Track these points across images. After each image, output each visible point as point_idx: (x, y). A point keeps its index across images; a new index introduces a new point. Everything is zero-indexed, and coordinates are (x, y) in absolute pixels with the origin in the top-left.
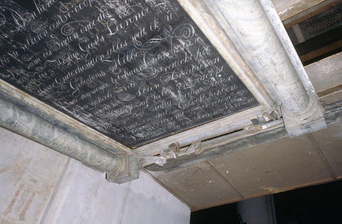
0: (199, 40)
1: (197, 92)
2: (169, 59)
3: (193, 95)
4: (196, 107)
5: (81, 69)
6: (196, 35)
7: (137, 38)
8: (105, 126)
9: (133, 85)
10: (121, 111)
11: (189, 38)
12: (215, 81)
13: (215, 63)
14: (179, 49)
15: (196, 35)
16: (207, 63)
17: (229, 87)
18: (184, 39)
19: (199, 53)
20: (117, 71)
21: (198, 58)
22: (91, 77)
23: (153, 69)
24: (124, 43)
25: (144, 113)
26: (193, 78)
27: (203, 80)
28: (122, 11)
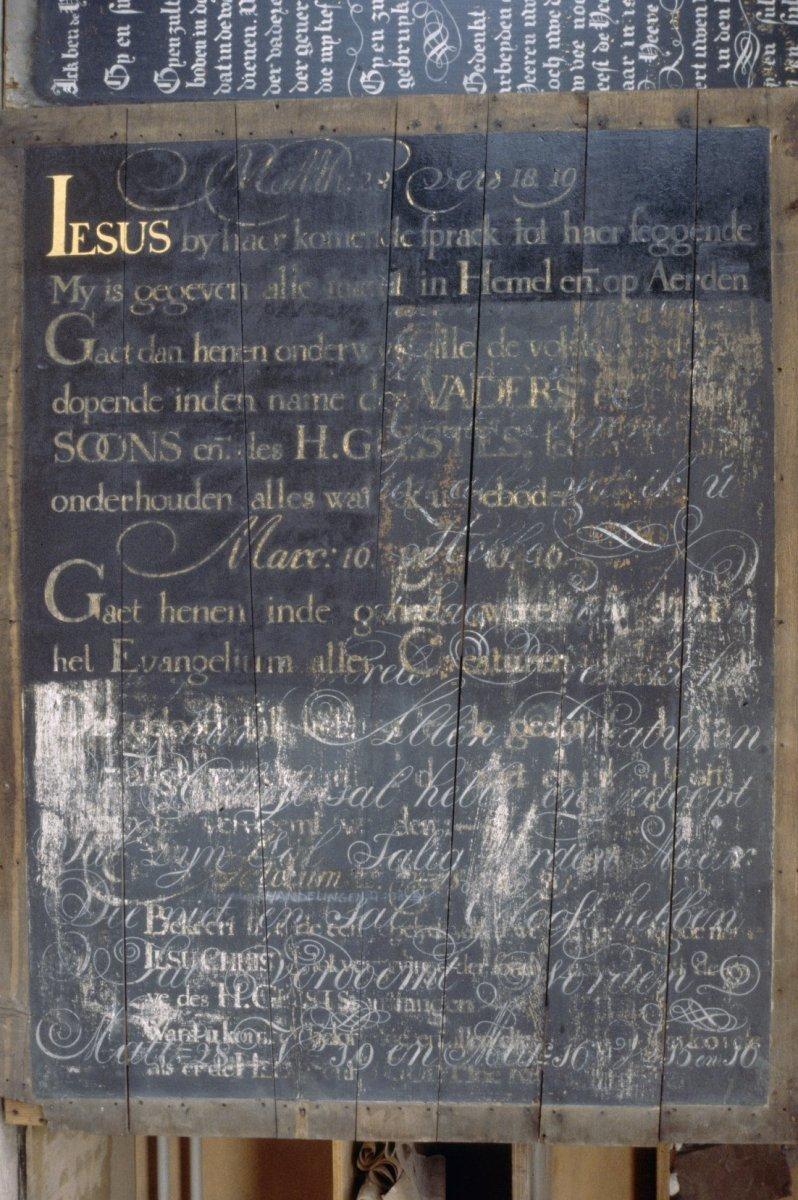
0: (749, 616)
1: (586, 864)
6: (749, 593)
11: (722, 592)
12: (684, 843)
13: (736, 747)
15: (749, 593)
17: (712, 909)
18: (706, 589)
19: (716, 669)
20: (414, 575)
23: (533, 642)
26: (622, 780)
27: (652, 808)
28: (616, 385)
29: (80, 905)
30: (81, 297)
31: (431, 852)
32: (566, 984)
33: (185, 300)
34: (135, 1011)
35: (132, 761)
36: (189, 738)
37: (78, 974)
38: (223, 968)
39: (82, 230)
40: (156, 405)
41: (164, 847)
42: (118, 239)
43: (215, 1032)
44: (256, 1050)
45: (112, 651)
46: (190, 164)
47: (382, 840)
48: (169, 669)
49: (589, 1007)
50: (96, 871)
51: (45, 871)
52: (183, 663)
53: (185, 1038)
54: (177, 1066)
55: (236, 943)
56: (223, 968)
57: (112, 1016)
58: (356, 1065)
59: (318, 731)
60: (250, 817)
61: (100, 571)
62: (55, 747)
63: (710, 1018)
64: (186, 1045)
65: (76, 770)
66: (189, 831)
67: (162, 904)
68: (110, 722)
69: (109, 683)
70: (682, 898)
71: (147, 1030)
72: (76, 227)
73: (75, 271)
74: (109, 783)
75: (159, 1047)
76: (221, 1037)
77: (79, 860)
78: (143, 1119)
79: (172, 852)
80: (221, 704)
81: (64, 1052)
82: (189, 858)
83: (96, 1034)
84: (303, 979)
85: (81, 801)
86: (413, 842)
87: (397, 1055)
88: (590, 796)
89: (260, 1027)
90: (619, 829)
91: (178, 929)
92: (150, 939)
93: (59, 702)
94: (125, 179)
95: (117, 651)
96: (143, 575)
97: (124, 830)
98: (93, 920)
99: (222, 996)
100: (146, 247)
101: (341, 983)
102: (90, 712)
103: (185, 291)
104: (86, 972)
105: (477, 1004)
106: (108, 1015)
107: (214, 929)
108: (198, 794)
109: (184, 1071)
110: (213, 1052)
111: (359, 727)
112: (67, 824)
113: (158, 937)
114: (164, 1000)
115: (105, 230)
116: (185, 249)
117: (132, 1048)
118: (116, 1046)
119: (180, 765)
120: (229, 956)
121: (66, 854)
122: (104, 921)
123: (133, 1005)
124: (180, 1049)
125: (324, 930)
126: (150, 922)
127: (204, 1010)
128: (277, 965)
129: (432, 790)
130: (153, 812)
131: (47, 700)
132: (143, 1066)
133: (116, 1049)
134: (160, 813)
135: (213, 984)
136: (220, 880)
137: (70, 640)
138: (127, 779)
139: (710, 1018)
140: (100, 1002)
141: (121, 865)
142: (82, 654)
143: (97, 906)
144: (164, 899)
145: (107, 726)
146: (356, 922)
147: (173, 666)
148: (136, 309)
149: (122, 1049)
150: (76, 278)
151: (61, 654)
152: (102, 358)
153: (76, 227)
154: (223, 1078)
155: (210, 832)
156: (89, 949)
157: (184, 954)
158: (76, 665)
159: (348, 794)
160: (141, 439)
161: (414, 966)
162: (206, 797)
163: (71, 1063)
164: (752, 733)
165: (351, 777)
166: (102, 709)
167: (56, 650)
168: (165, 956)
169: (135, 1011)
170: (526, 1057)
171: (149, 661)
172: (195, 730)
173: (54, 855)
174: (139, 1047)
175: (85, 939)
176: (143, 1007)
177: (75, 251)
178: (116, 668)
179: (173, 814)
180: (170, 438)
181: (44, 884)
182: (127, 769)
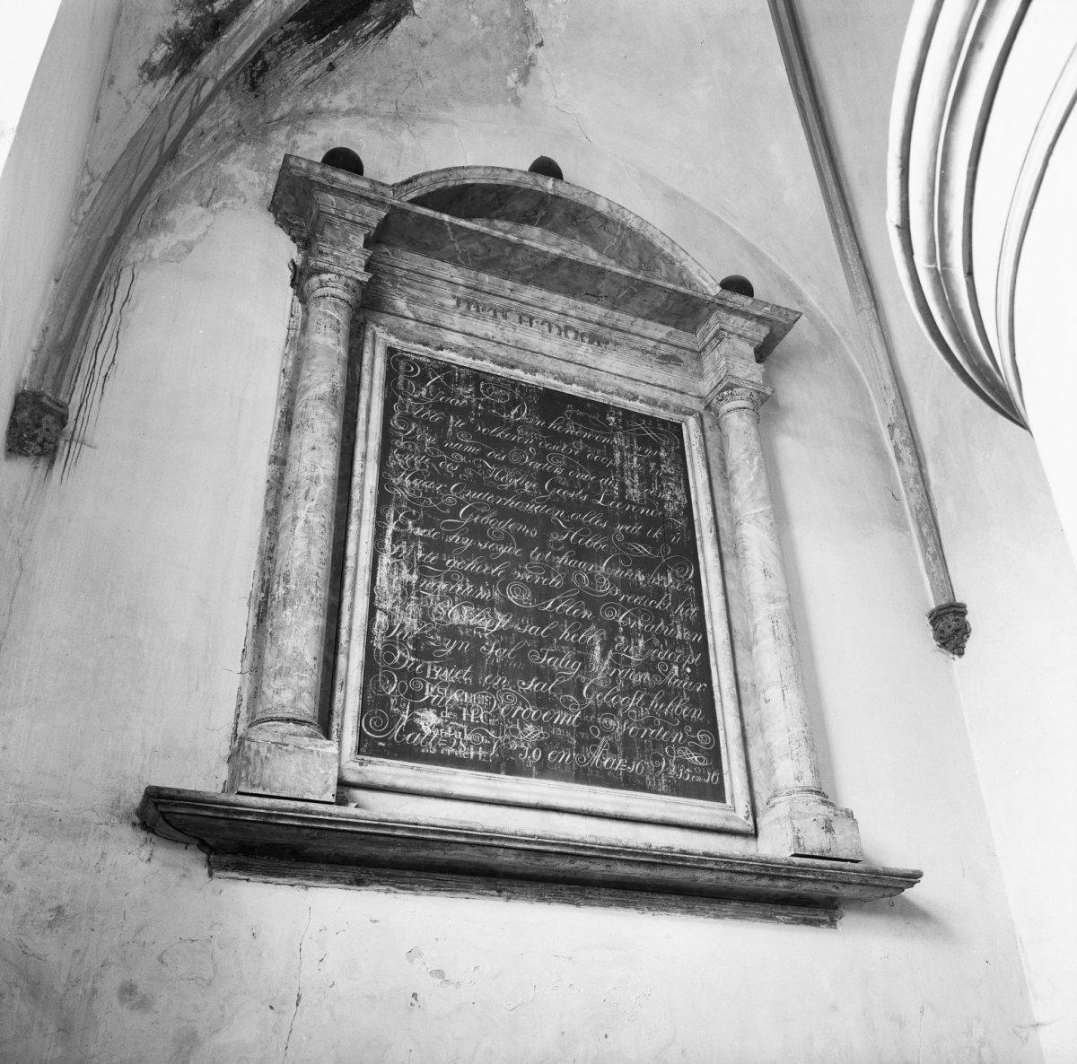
1: (636, 678)
2: (639, 585)
3: (627, 681)
4: (612, 718)
5: (511, 503)
7: (623, 530)
8: (403, 625)
9: (554, 583)
10: (478, 615)
14: (662, 582)
16: (683, 632)
18: (674, 575)
20: (557, 544)
21: (676, 615)
22: (510, 524)
24: (603, 522)
25: (512, 655)
26: (649, 645)
31: (566, 661)
32: (631, 731)
36: (453, 590)
37: (389, 693)
41: (439, 638)
44: (482, 745)
47: (545, 651)
49: (642, 746)
54: (439, 749)
55: (474, 688)
58: (532, 759)
59: (514, 599)
60: (482, 631)
63: (696, 758)
66: (451, 632)
68: (415, 577)
70: (677, 701)
71: (423, 727)
74: (412, 604)
75: (429, 737)
76: (463, 736)
77: (394, 637)
79: (442, 641)
82: (451, 644)
84: (506, 712)
85: (397, 608)
86: (559, 655)
87: (553, 756)
88: (635, 649)
89: (484, 733)
90: (648, 665)
92: (428, 679)
97: (419, 626)
99: (464, 714)
101: (525, 717)
102: (405, 571)
105: (590, 736)
106: (403, 716)
107: (462, 680)
110: (459, 744)
111: (533, 601)
112: (389, 618)
117: (415, 736)
118: (407, 734)
120: (469, 694)
122: (405, 668)
125: (516, 689)
126: (429, 672)
128: (493, 704)
129: (566, 634)
139: (696, 758)
141: (416, 642)
146: (532, 687)
149: (410, 736)
159: (528, 629)
161: (560, 713)
163: (381, 740)
164: (699, 636)
165: (530, 621)
168: (436, 690)
170: (615, 765)
176: (422, 715)
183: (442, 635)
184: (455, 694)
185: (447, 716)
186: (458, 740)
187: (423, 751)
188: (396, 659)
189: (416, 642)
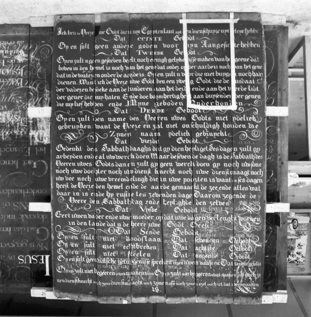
29: (39, 86)
30: (41, 245)
33: (14, 243)
34: (26, 58)
35: (25, 124)
36: (10, 130)
38: (3, 70)
39: (41, 261)
40: (20, 216)
41: (17, 102)
42: (32, 259)
43: (6, 53)
45: (30, 153)
46: (14, 278)
48: (16, 148)
50: (35, 95)
51: (48, 95)
52: (12, 150)
53: (14, 51)
54: (16, 44)
56: (3, 70)
57: (32, 56)
61: (33, 173)
62: (45, 127)
64: (13, 49)
65: (40, 121)
67: (18, 87)
69: (31, 144)
71: (23, 53)
72: (43, 262)
73: (42, 251)
75: (20, 48)
76: (4, 52)
77: (39, 98)
78: (26, 29)
79: (15, 100)
80: (2, 139)
81: (46, 46)
82: (11, 99)
83: (37, 51)
91: (14, 80)
92: (22, 77)
93: (44, 139)
94: (31, 273)
95: (29, 153)
96: (22, 173)
98: (36, 82)
100: (24, 257)
103: (14, 245)
104: (38, 68)
106: (33, 57)
107: (5, 80)
108: (8, 116)
109: (14, 42)
113: (19, 78)
114: (18, 61)
115: (35, 261)
116: (14, 256)
118: (32, 48)
119: (13, 123)
121: (43, 99)
122: (33, 82)
123: (26, 59)
124: (15, 48)
126: (21, 82)
127: (8, 59)
130: (20, 111)
131: (47, 140)
132: (25, 43)
133: (32, 48)
134: (18, 110)
135: (6, 66)
136: (3, 93)
137: (41, 156)
138: (26, 119)
140: (35, 60)
141: (29, 96)
142: (38, 152)
143: (35, 86)
144: (18, 88)
145: (32, 133)
147: (14, 149)
148: (26, 241)
150: (42, 249)
151: (44, 152)
152: (34, 229)
153: (43, 262)
154: (4, 41)
155: (5, 106)
156: (37, 74)
157: (13, 73)
158: (40, 149)
160: (24, 208)
162: (6, 115)
163: (44, 44)
166: (33, 138)
167: (45, 153)
168: (18, 73)
169: (26, 58)
171: (21, 150)
172: (9, 132)
173: (46, 99)
174: (26, 48)
175: (38, 77)
176: (24, 59)
177: (43, 256)
178: (29, 148)
179: (15, 110)
180: (16, 208)
181: (49, 91)
182: (27, 122)
183: (15, 103)
184: (8, 72)
185: (12, 61)
186: (6, 49)
187: (23, 42)
188: (38, 85)
189: (29, 96)
